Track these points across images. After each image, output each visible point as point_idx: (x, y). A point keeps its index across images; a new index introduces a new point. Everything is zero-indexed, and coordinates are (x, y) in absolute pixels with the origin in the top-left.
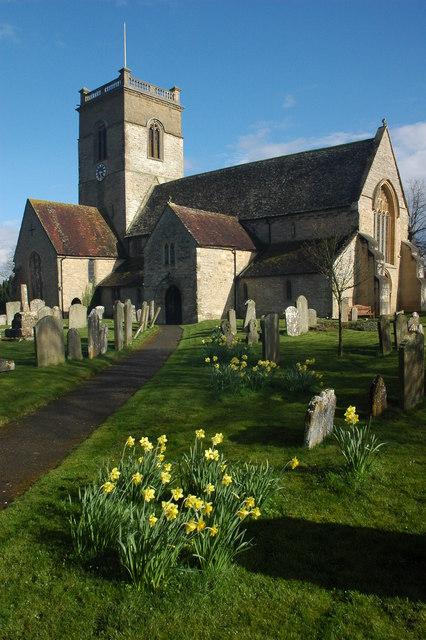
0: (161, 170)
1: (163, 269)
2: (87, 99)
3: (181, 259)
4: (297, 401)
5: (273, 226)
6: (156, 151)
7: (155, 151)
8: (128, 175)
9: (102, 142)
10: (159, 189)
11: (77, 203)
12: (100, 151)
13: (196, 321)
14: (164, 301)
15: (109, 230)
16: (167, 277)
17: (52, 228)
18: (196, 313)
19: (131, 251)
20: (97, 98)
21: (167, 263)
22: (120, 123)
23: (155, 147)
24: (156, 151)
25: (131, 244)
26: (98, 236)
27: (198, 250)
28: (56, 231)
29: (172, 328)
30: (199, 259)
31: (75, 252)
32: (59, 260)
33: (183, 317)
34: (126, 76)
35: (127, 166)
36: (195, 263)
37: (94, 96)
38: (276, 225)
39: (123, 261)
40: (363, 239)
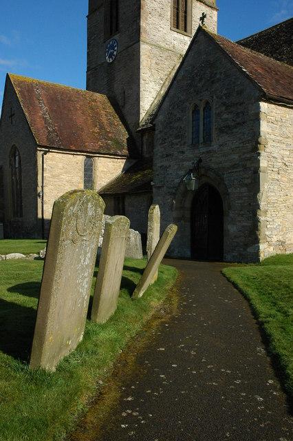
1: (189, 154)
3: (225, 129)
8: (144, 48)
9: (115, 14)
12: (111, 22)
13: (254, 258)
14: (188, 215)
15: (117, 121)
18: (256, 241)
19: (145, 147)
23: (181, 14)
25: (145, 138)
26: (102, 127)
28: (39, 118)
29: (203, 268)
30: (264, 127)
31: (67, 146)
32: (40, 154)
33: (227, 243)
35: (143, 36)
36: (256, 134)
39: (134, 161)
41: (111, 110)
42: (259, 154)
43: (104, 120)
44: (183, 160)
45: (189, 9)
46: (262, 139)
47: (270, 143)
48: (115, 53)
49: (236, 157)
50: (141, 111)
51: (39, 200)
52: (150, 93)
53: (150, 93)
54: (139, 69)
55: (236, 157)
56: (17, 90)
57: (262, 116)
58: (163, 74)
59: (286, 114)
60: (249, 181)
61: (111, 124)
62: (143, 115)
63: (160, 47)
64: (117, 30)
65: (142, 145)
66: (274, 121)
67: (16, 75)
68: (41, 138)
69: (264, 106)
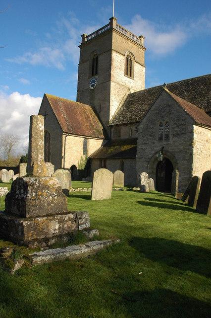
0: (132, 85)
2: (86, 40)
6: (129, 73)
7: (129, 72)
8: (112, 84)
10: (130, 95)
11: (75, 100)
12: (93, 69)
15: (97, 120)
16: (162, 149)
17: (60, 114)
19: (112, 134)
20: (95, 37)
22: (109, 51)
23: (129, 68)
24: (129, 73)
25: (113, 130)
26: (90, 123)
27: (195, 127)
28: (62, 117)
31: (76, 132)
32: (64, 136)
34: (114, 22)
39: (106, 141)
41: (93, 114)
42: (193, 147)
43: (91, 118)
44: (153, 147)
45: (132, 67)
46: (194, 141)
47: (197, 142)
48: (95, 85)
50: (110, 116)
51: (63, 160)
52: (115, 106)
53: (115, 106)
54: (109, 94)
55: (182, 147)
56: (50, 102)
57: (194, 131)
58: (121, 98)
59: (207, 133)
60: (188, 158)
61: (94, 122)
62: (111, 118)
64: (96, 73)
65: (111, 133)
66: (201, 135)
67: (49, 95)
68: (65, 128)
69: (195, 127)
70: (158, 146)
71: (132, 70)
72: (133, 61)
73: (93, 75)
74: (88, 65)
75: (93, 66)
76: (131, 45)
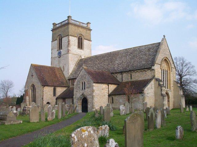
0: (83, 53)
3: (88, 88)
4: (55, 117)
5: (123, 75)
7: (80, 45)
10: (81, 60)
16: (83, 94)
19: (70, 84)
21: (82, 89)
25: (70, 81)
30: (94, 88)
37: (57, 26)
38: (124, 75)
40: (157, 80)
49: (90, 93)
63: (74, 54)
70: (81, 92)
71: (83, 44)
72: (83, 39)
73: (59, 49)
74: (56, 42)
75: (60, 43)
76: (81, 29)
